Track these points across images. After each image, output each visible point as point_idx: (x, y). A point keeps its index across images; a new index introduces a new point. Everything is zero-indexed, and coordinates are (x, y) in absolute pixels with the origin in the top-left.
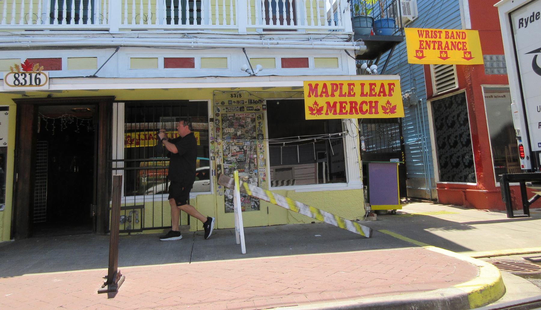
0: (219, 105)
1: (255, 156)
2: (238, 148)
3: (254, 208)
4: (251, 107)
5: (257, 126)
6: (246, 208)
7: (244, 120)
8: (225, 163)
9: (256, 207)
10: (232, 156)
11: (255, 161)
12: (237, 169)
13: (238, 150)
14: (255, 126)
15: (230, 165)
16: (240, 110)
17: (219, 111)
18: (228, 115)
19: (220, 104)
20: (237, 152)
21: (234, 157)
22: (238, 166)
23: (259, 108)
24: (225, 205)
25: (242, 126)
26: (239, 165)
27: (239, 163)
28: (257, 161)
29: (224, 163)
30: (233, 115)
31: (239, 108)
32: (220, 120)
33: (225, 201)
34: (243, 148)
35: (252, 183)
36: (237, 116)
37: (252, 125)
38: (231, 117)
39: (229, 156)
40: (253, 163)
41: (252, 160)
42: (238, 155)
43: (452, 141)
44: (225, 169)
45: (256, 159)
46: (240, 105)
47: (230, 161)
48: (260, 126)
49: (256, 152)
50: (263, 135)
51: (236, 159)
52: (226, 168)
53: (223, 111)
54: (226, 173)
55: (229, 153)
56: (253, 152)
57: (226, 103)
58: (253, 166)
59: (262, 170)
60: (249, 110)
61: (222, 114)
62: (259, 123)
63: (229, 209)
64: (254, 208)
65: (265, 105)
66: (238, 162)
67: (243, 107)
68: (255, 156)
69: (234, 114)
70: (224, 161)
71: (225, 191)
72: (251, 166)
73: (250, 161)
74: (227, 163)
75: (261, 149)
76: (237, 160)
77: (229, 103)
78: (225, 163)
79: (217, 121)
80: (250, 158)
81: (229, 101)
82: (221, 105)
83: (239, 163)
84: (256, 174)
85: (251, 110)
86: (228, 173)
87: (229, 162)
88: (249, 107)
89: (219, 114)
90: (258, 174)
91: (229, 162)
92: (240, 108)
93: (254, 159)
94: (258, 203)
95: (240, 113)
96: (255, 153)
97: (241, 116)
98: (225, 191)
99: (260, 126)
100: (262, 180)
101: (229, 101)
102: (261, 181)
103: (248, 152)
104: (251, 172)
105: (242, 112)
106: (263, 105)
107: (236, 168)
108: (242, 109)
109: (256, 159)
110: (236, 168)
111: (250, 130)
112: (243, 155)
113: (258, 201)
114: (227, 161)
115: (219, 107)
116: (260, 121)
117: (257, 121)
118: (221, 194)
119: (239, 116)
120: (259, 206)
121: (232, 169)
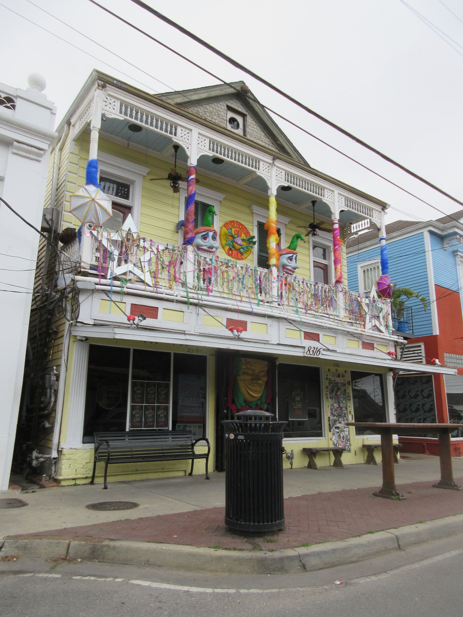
1: (346, 412)
10: (335, 410)
13: (338, 406)
20: (337, 408)
34: (339, 406)
37: (344, 388)
40: (345, 417)
43: (414, 407)
48: (348, 390)
49: (346, 409)
50: (350, 396)
66: (338, 415)
68: (346, 412)
70: (332, 414)
75: (349, 407)
95: (337, 379)
97: (338, 381)
103: (344, 409)
108: (339, 376)
117: (347, 386)
120: (350, 449)
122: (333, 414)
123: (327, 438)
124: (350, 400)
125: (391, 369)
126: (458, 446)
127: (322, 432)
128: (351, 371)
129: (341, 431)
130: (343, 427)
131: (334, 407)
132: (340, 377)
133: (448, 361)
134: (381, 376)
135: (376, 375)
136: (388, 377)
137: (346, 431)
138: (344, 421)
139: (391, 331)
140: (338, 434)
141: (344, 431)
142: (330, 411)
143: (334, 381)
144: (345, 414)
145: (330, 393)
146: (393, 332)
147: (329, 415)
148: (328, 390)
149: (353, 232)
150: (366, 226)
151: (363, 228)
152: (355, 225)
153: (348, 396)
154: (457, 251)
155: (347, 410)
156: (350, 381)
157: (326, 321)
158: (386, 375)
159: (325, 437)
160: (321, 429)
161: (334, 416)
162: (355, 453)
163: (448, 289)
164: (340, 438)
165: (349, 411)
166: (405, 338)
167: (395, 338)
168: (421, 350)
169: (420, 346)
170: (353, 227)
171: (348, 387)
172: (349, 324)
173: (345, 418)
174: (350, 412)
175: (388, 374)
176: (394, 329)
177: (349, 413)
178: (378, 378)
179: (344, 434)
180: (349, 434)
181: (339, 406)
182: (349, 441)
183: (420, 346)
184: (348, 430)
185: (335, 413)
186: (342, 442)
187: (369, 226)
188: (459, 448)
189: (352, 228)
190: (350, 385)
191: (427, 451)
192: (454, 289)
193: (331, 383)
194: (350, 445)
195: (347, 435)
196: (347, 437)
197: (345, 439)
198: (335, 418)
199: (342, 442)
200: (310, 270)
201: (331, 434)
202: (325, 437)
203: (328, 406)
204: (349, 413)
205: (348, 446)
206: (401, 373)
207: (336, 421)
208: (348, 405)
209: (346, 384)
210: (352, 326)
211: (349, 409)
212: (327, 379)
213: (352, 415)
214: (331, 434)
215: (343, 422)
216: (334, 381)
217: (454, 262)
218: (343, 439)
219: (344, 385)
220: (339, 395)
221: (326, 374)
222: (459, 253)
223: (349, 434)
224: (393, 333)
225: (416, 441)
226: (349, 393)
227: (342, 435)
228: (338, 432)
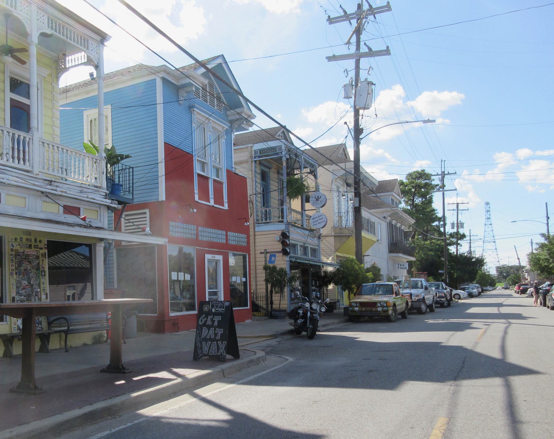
0: (13, 241)
1: (39, 290)
2: (27, 282)
4: (37, 245)
5: (41, 263)
7: (31, 257)
10: (23, 289)
13: (27, 283)
14: (39, 263)
15: (21, 297)
16: (29, 248)
17: (13, 247)
18: (20, 251)
19: (14, 240)
20: (26, 286)
21: (24, 291)
23: (42, 247)
25: (30, 262)
30: (23, 251)
31: (28, 245)
32: (14, 255)
34: (29, 283)
36: (26, 253)
37: (37, 262)
38: (21, 253)
39: (20, 289)
40: (37, 296)
45: (39, 293)
46: (29, 243)
47: (21, 293)
48: (43, 263)
50: (45, 272)
51: (25, 292)
53: (16, 247)
55: (20, 287)
57: (19, 240)
60: (36, 248)
61: (15, 250)
62: (43, 260)
65: (46, 245)
67: (31, 245)
68: (39, 290)
69: (24, 251)
70: (18, 293)
73: (35, 294)
74: (19, 296)
75: (43, 284)
77: (20, 240)
79: (12, 256)
80: (36, 292)
81: (20, 238)
82: (15, 241)
85: (37, 248)
88: (36, 245)
89: (13, 249)
92: (29, 245)
93: (38, 293)
95: (28, 250)
97: (29, 253)
99: (43, 263)
101: (20, 238)
103: (35, 286)
105: (30, 249)
106: (45, 245)
107: (25, 300)
108: (30, 247)
109: (39, 293)
110: (25, 300)
111: (35, 266)
114: (19, 293)
115: (13, 243)
116: (43, 259)
117: (41, 259)
119: (27, 252)
124: (45, 275)
125: (101, 240)
126: (177, 322)
128: (47, 240)
131: (21, 284)
132: (31, 248)
133: (174, 230)
134: (90, 246)
135: (87, 245)
136: (97, 248)
139: (104, 194)
142: (15, 289)
143: (24, 252)
144: (37, 292)
145: (16, 267)
146: (106, 195)
147: (14, 294)
148: (14, 264)
149: (67, 66)
150: (83, 61)
151: (80, 63)
152: (70, 58)
153: (42, 271)
154: (193, 106)
156: (45, 253)
157: (10, 177)
158: (95, 245)
159: (6, 321)
161: (21, 296)
163: (177, 148)
165: (42, 288)
166: (120, 203)
167: (108, 202)
168: (146, 217)
169: (145, 213)
170: (68, 60)
171: (43, 260)
172: (47, 182)
173: (37, 298)
174: (43, 289)
175: (98, 244)
176: (108, 192)
178: (88, 249)
181: (29, 283)
183: (145, 213)
185: (23, 292)
187: (86, 61)
188: (178, 323)
189: (67, 62)
190: (45, 258)
192: (188, 150)
193: (19, 255)
198: (23, 297)
200: (4, 110)
202: (6, 321)
203: (13, 285)
204: (42, 293)
206: (123, 243)
208: (42, 280)
209: (40, 256)
210: (51, 185)
211: (42, 286)
212: (12, 250)
216: (24, 252)
217: (189, 118)
219: (38, 257)
220: (30, 270)
221: (11, 244)
222: (195, 109)
224: (106, 196)
226: (43, 268)
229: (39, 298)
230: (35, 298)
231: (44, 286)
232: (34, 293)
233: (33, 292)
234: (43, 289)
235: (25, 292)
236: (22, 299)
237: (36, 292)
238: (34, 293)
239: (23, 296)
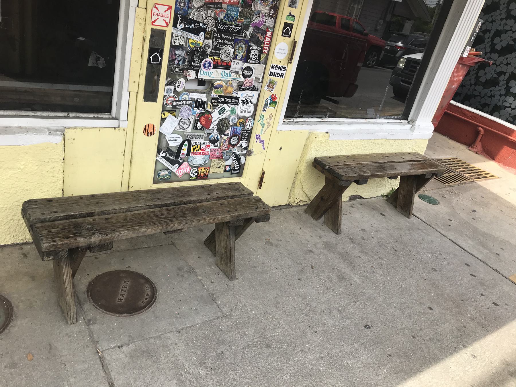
3: (229, 171)
6: (211, 172)
8: (181, 26)
9: (235, 170)
11: (265, 38)
12: (213, 54)
21: (211, 13)
22: (215, 44)
24: (156, 160)
26: (219, 43)
27: (221, 35)
28: (270, 42)
29: (175, 25)
33: (159, 151)
35: (241, 104)
40: (259, 43)
41: (259, 35)
42: (225, 6)
44: (173, 47)
51: (216, 19)
52: (177, 44)
54: (176, 62)
56: (268, 8)
58: (257, 52)
59: (277, 71)
63: (166, 172)
64: (229, 171)
66: (220, 31)
68: (270, 22)
71: (163, 120)
72: (253, 52)
73: (252, 35)
74: (185, 29)
76: (216, 26)
78: (181, 26)
80: (257, 28)
83: (221, 35)
84: (259, 79)
86: (181, 63)
87: (192, 26)
90: (262, 82)
91: (192, 26)
93: (264, 33)
94: (242, 158)
96: (272, 12)
98: (163, 120)
100: (269, 101)
102: (266, 104)
104: (246, 73)
107: (209, 51)
109: (269, 34)
110: (209, 51)
112: (240, 9)
113: (243, 155)
114: (186, 19)
118: (151, 130)
121: (198, 52)
122: (192, 22)
123: (124, 124)
127: (111, 94)
129: (216, 102)
130: (235, 87)
137: (246, 102)
138: (246, 59)
140: (199, 111)
141: (233, 100)
155: (275, 16)
160: (111, 84)
161: (196, 32)
162: (261, 180)
164: (206, 126)
165: (283, 18)
173: (255, 50)
174: (286, 25)
177: (279, 29)
179: (233, 112)
180: (254, 116)
182: (248, 140)
184: (254, 101)
186: (214, 141)
191: (478, 145)
194: (249, 153)
195: (246, 119)
196: (243, 125)
197: (229, 131)
198: (200, 39)
199: (214, 141)
201: (157, 106)
205: (238, 158)
207: (204, 54)
213: (295, 43)
214: (157, 106)
215: (238, 65)
218: (221, 131)
223: (254, 116)
225: (466, 116)
227: (216, 116)
228: (200, 104)
229: (261, 52)
230: (249, 51)
231: (294, 12)
232: (251, 29)
233: (246, 28)
234: (286, 25)
235: (216, 19)
236: (197, 45)
237: (257, 28)
238: (251, 29)
239: (202, 34)
